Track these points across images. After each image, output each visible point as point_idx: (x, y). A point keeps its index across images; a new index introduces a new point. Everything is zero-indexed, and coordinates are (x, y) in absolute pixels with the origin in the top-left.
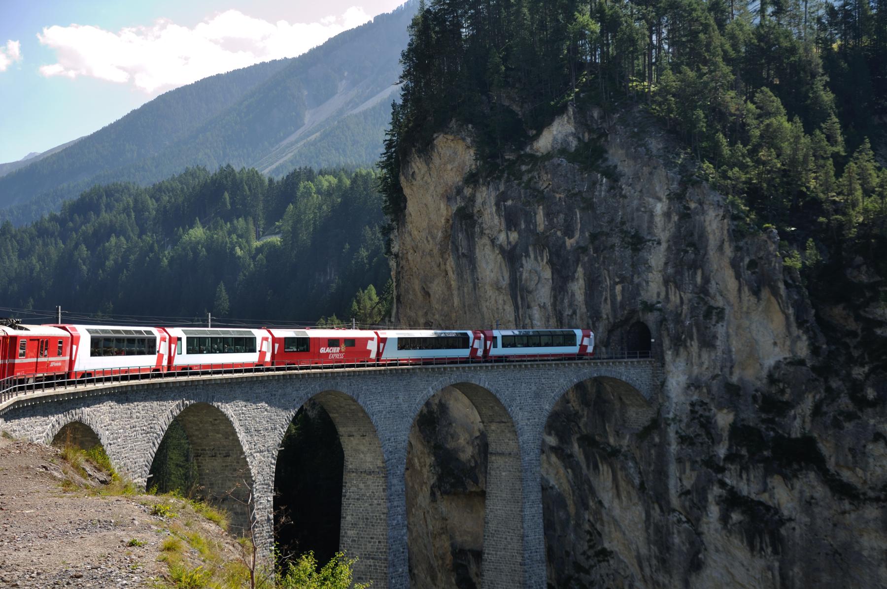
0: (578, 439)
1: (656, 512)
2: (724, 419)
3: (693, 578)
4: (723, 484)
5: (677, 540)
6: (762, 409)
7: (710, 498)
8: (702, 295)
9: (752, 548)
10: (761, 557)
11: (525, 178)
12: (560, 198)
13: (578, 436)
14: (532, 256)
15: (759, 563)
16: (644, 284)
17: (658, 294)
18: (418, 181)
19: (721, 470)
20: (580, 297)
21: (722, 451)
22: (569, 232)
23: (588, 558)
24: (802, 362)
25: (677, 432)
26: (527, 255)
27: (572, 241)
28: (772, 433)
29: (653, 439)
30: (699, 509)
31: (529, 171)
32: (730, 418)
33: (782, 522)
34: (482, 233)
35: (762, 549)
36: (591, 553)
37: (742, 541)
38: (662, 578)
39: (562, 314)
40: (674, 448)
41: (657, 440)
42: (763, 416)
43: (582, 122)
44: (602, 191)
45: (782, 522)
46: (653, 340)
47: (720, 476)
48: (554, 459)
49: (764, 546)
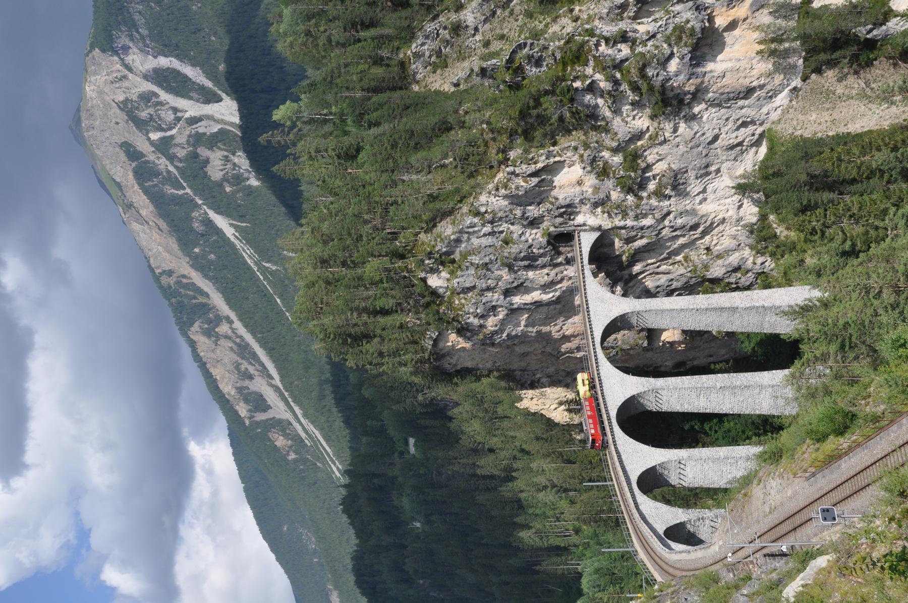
0: (621, 271)
1: (664, 232)
3: (701, 213)
5: (679, 221)
6: (608, 176)
7: (657, 204)
9: (683, 184)
11: (463, 301)
13: (618, 272)
15: (692, 180)
16: (532, 236)
18: (453, 361)
22: (499, 279)
24: (582, 156)
31: (459, 300)
33: (670, 169)
36: (685, 264)
38: (701, 229)
41: (623, 231)
42: (611, 175)
43: (432, 271)
44: (476, 259)
45: (670, 169)
48: (631, 284)
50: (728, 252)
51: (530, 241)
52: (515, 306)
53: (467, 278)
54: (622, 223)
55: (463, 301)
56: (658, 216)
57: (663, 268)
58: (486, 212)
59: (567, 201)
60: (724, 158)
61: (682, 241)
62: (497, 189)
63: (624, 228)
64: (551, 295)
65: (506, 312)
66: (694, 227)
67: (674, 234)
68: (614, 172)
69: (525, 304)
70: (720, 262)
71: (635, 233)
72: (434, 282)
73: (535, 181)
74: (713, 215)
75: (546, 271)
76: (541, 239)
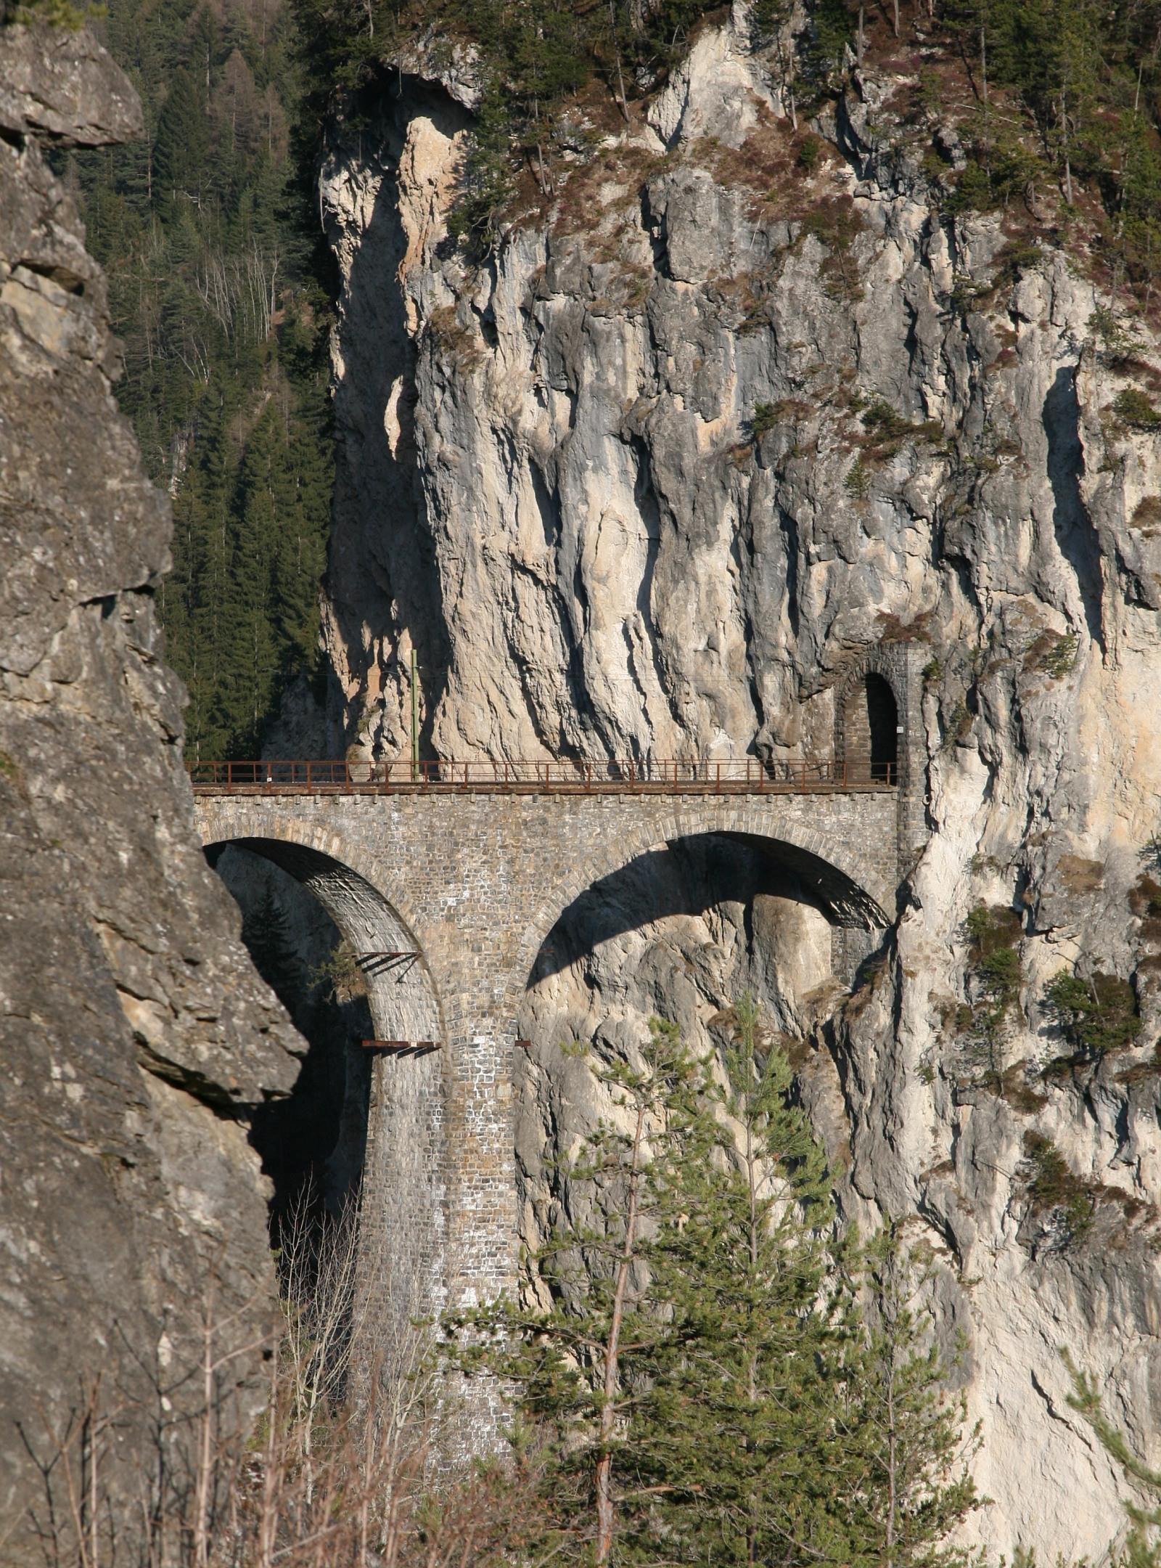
4: (1036, 1144)
8: (1031, 598)
10: (1110, 1344)
11: (607, 226)
12: (686, 293)
14: (614, 469)
16: (893, 562)
17: (926, 590)
19: (1031, 1103)
20: (727, 599)
26: (600, 467)
27: (715, 425)
30: (970, 1212)
31: (620, 204)
32: (1071, 951)
35: (1112, 1316)
37: (1064, 1299)
39: (678, 648)
40: (921, 1038)
41: (885, 1019)
46: (900, 730)
47: (1028, 1121)
49: (1118, 1311)
51: (867, 547)
52: (570, 495)
54: (919, 1007)
55: (607, 226)
56: (943, 1191)
59: (1035, 730)
62: (1120, 365)
64: (619, 673)
65: (549, 443)
71: (871, 1076)
75: (731, 638)
76: (872, 608)
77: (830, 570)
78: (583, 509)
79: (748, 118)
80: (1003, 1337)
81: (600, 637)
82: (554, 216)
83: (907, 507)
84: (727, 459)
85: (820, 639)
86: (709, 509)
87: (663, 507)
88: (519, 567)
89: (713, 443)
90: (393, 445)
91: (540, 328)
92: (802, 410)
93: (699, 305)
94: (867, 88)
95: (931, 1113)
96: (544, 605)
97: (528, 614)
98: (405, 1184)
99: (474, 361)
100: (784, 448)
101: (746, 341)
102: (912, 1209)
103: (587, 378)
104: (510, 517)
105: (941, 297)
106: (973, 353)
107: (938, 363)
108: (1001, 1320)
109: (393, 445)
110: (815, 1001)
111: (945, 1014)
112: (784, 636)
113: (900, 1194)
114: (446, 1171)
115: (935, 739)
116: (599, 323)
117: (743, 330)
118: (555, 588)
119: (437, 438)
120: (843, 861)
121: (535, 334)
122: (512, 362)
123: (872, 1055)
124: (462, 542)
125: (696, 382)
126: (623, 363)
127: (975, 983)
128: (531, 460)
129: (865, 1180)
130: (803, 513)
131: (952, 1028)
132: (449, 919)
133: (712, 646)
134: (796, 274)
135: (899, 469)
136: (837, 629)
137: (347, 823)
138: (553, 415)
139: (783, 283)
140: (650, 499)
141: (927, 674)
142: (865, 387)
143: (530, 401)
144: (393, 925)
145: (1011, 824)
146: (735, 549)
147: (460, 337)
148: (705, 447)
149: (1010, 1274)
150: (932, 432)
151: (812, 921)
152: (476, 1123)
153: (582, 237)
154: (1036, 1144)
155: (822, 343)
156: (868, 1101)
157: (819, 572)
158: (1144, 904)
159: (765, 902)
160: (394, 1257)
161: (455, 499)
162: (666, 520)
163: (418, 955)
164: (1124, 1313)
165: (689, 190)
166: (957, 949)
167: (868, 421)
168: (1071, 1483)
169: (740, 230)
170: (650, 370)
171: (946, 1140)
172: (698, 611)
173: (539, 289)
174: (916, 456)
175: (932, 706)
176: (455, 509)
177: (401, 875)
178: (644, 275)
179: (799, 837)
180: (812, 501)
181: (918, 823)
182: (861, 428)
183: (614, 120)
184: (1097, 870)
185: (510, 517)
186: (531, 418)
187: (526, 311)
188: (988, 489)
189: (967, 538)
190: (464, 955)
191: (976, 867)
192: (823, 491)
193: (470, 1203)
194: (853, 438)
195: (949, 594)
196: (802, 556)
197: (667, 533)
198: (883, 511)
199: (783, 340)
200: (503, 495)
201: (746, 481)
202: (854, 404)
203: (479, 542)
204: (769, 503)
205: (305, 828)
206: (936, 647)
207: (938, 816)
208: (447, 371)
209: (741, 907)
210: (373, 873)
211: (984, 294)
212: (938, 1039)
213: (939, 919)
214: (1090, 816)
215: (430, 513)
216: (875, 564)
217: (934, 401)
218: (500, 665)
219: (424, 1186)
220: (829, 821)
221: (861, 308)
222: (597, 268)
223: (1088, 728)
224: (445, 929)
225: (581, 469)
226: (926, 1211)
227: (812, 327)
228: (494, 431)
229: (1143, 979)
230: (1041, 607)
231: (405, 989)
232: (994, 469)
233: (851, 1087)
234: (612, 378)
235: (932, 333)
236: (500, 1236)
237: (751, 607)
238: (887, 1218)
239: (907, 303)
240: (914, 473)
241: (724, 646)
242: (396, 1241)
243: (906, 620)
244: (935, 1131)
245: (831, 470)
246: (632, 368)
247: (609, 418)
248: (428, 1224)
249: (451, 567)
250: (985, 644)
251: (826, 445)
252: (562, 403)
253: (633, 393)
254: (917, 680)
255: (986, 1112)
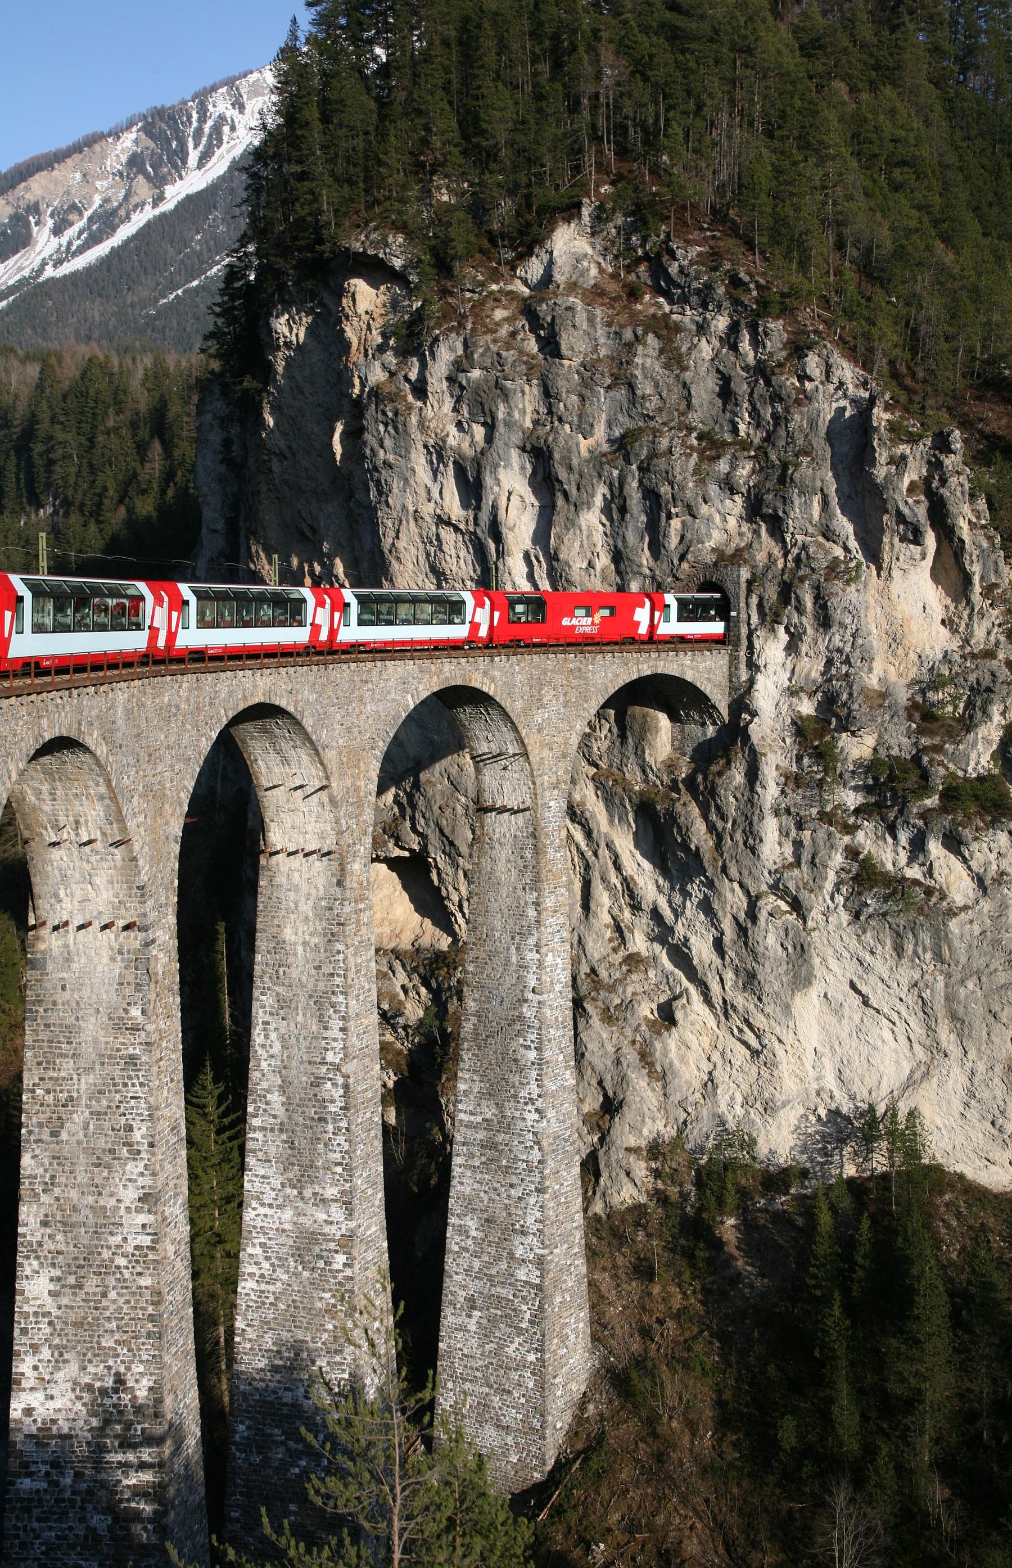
2: (857, 748)
4: (852, 853)
6: (920, 732)
8: (821, 539)
9: (899, 950)
14: (516, 467)
16: (717, 518)
19: (850, 830)
21: (852, 799)
23: (611, 965)
25: (777, 767)
27: (591, 441)
28: (942, 771)
29: (731, 778)
32: (870, 741)
34: (422, 426)
35: (915, 952)
38: (740, 1000)
42: (925, 741)
44: (647, 358)
46: (733, 614)
47: (847, 839)
49: (920, 950)
50: (661, 1076)
51: (704, 509)
53: (585, 335)
55: (504, 331)
56: (793, 879)
57: (602, 898)
58: (804, 377)
59: (837, 615)
60: (981, 1067)
61: (701, 949)
63: (753, 774)
65: (470, 453)
66: (750, 980)
67: (727, 925)
68: (938, 749)
69: (495, 507)
70: (631, 1056)
71: (732, 812)
72: (570, 244)
73: (921, 512)
74: (788, 1038)
75: (604, 561)
77: (683, 523)
78: (496, 489)
79: (594, 271)
80: (833, 963)
81: (510, 561)
82: (469, 326)
83: (729, 486)
84: (598, 460)
85: (676, 562)
86: (589, 489)
87: (557, 486)
88: (442, 521)
89: (590, 452)
90: (338, 457)
91: (462, 388)
92: (656, 433)
93: (578, 372)
94: (679, 253)
95: (777, 834)
96: (461, 545)
97: (449, 548)
98: (504, 891)
99: (410, 408)
100: (644, 453)
101: (612, 393)
102: (764, 888)
103: (501, 415)
104: (436, 495)
105: (746, 368)
106: (776, 397)
107: (746, 405)
108: (830, 952)
109: (338, 457)
110: (670, 766)
111: (787, 778)
112: (645, 558)
113: (756, 879)
114: (536, 884)
115: (755, 619)
116: (508, 384)
117: (609, 388)
118: (475, 533)
119: (381, 452)
120: (706, 688)
121: (457, 392)
122: (440, 409)
123: (732, 799)
124: (399, 507)
125: (580, 417)
126: (525, 405)
127: (806, 761)
128: (455, 463)
129: (733, 871)
130: (665, 490)
131: (791, 785)
132: (539, 731)
133: (591, 565)
134: (646, 355)
135: (723, 466)
136: (689, 556)
137: (497, 674)
138: (472, 437)
139: (638, 360)
140: (545, 482)
141: (749, 583)
142: (695, 418)
143: (453, 430)
144: (510, 736)
145: (812, 668)
146: (606, 510)
147: (395, 397)
148: (584, 453)
149: (839, 926)
150: (745, 445)
151: (663, 720)
152: (551, 853)
153: (488, 338)
154: (852, 853)
155: (664, 394)
156: (729, 825)
157: (676, 524)
158: (917, 716)
159: (637, 710)
160: (497, 934)
161: (396, 485)
162: (559, 495)
163: (525, 754)
164: (925, 951)
165: (569, 309)
166: (788, 740)
167: (699, 438)
168: (879, 1043)
169: (601, 332)
170: (543, 410)
171: (788, 849)
172: (582, 546)
173: (459, 366)
174: (735, 457)
175: (754, 600)
176: (395, 491)
177: (519, 705)
178: (533, 357)
179: (689, 677)
180: (671, 484)
181: (743, 666)
182: (695, 442)
183: (495, 276)
184: (883, 695)
185: (436, 495)
186: (454, 438)
187: (451, 379)
188: (797, 476)
189: (779, 504)
190: (546, 753)
191: (793, 692)
192: (679, 478)
193: (549, 902)
194: (691, 447)
195: (759, 536)
196: (663, 515)
197: (560, 502)
198: (713, 489)
199: (639, 393)
200: (430, 484)
201: (616, 473)
202: (690, 429)
203: (411, 509)
204: (635, 484)
205: (479, 678)
206: (753, 567)
207: (761, 662)
208: (390, 414)
209: (612, 712)
210: (506, 704)
211: (780, 365)
212: (783, 792)
213: (771, 723)
214: (875, 664)
215: (373, 494)
216: (709, 519)
217: (742, 428)
218: (421, 577)
219: (520, 893)
220: (702, 666)
221: (688, 375)
222: (504, 353)
223: (871, 613)
224: (537, 737)
225: (496, 466)
226: (777, 888)
227: (657, 385)
228: (426, 447)
229: (925, 759)
230: (828, 545)
231: (507, 774)
232: (797, 465)
233: (713, 817)
234: (517, 415)
235: (742, 389)
236: (562, 920)
237: (620, 544)
238: (748, 893)
239: (718, 371)
240: (733, 467)
241: (599, 565)
242: (498, 924)
243: (729, 551)
244: (780, 844)
245: (684, 467)
246: (529, 409)
247: (516, 438)
248: (523, 915)
249: (389, 523)
250: (791, 565)
251: (677, 451)
252: (479, 432)
253: (528, 424)
254: (744, 586)
255: (821, 834)
